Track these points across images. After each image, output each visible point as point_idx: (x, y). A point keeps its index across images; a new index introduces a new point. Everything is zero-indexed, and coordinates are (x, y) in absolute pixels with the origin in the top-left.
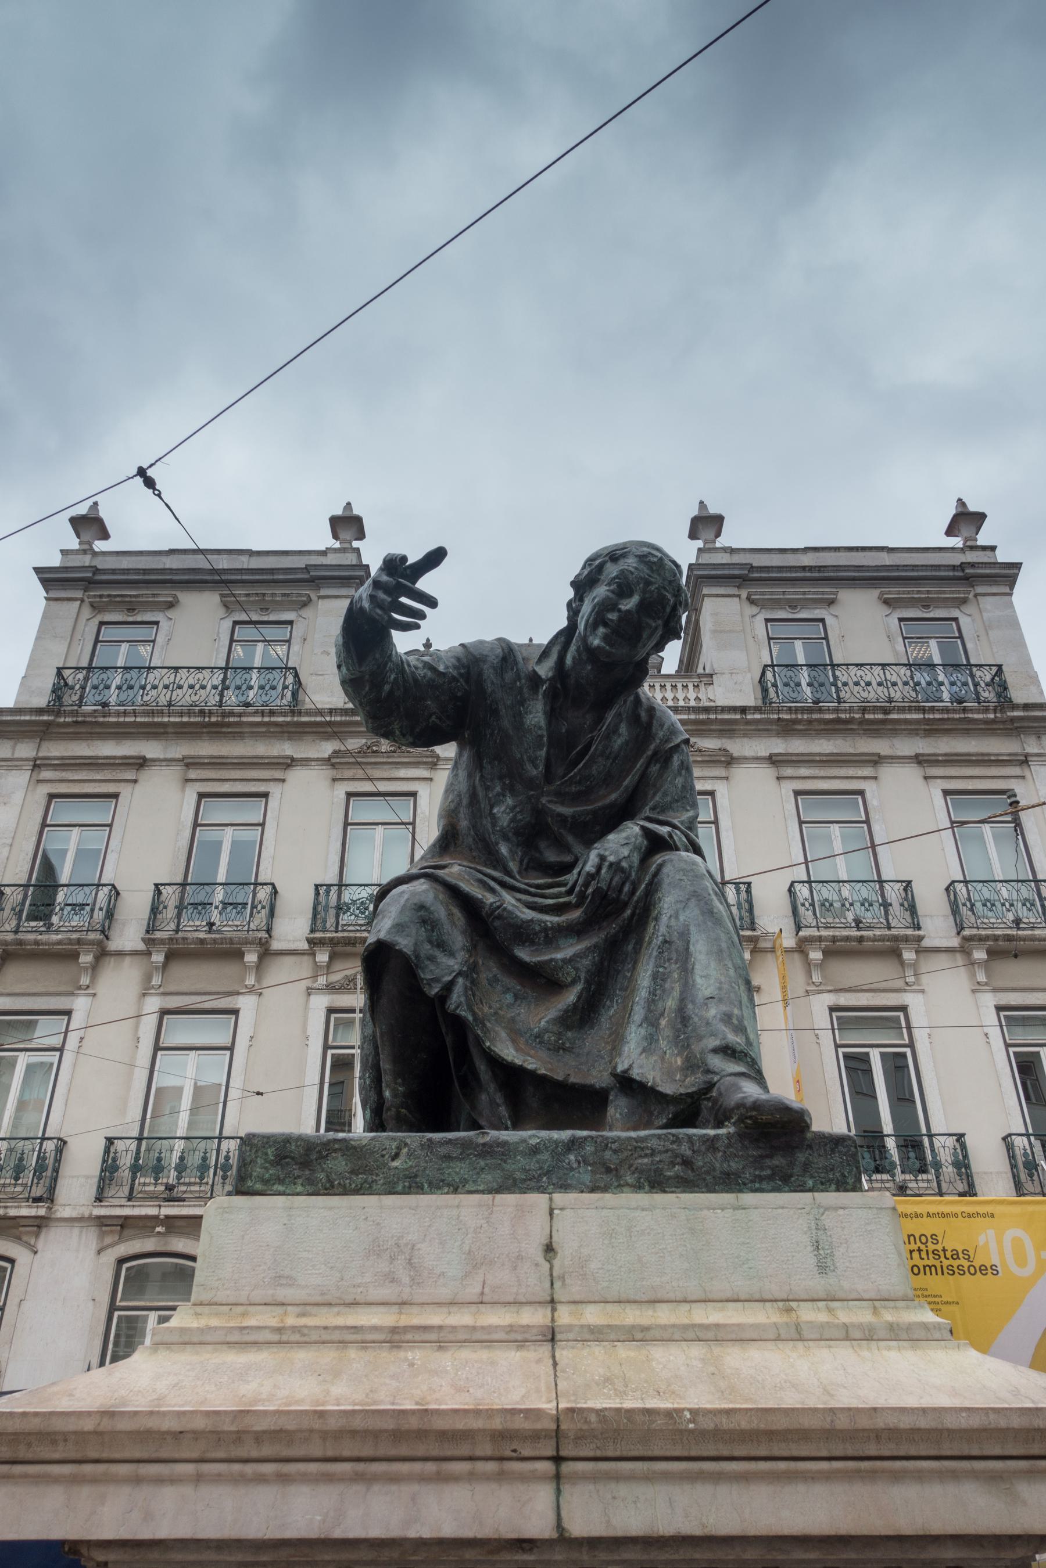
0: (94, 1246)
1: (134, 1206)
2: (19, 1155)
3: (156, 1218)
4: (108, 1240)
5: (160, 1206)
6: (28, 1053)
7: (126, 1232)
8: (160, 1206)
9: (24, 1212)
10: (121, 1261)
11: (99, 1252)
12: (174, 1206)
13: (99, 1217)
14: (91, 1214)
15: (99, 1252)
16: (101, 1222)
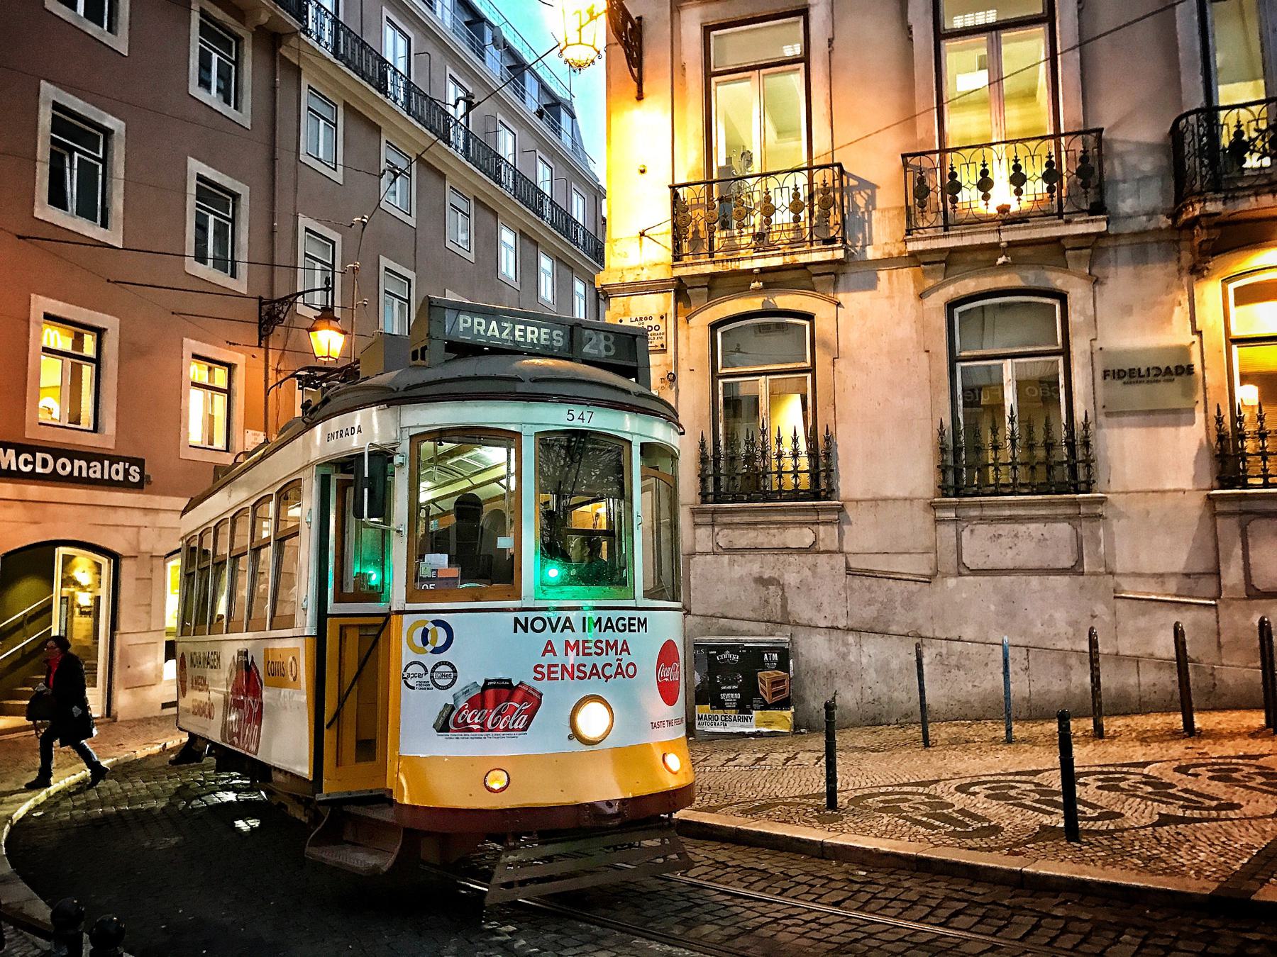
0: (911, 290)
1: (962, 235)
2: (792, 192)
3: (994, 247)
4: (930, 283)
5: (999, 231)
6: (762, 71)
7: (950, 271)
8: (999, 231)
9: (817, 257)
10: (951, 305)
11: (921, 296)
12: (1019, 229)
13: (913, 255)
14: (901, 253)
15: (921, 296)
16: (915, 259)
